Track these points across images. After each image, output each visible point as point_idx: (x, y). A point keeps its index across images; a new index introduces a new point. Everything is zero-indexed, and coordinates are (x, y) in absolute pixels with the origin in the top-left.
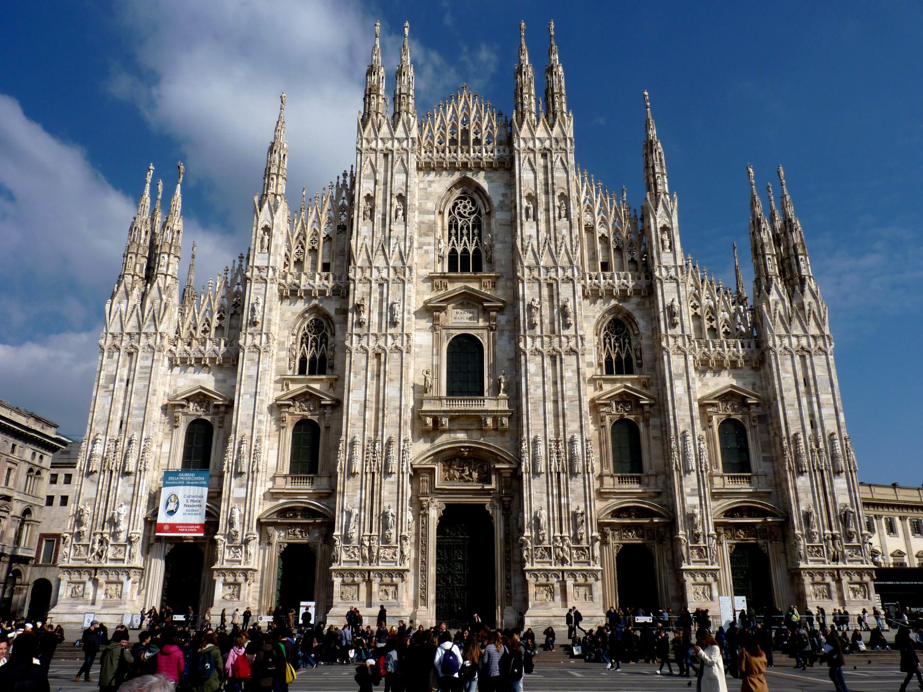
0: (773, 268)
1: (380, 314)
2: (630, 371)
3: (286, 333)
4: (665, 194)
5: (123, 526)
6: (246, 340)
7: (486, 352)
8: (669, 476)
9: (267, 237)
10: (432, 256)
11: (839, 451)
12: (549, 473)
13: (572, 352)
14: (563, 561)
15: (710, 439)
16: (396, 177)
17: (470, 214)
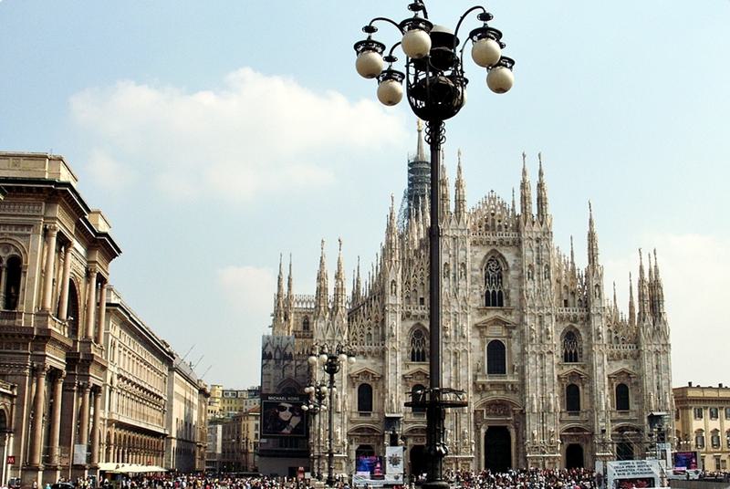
0: (647, 310)
1: (456, 331)
2: (576, 361)
3: (405, 338)
4: (598, 265)
5: (339, 438)
6: (389, 345)
7: (506, 350)
8: (592, 412)
9: (394, 287)
10: (478, 296)
11: (668, 401)
12: (538, 412)
13: (550, 353)
14: (544, 453)
15: (612, 394)
16: (460, 252)
17: (496, 270)
